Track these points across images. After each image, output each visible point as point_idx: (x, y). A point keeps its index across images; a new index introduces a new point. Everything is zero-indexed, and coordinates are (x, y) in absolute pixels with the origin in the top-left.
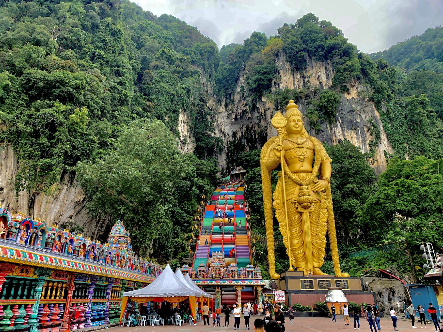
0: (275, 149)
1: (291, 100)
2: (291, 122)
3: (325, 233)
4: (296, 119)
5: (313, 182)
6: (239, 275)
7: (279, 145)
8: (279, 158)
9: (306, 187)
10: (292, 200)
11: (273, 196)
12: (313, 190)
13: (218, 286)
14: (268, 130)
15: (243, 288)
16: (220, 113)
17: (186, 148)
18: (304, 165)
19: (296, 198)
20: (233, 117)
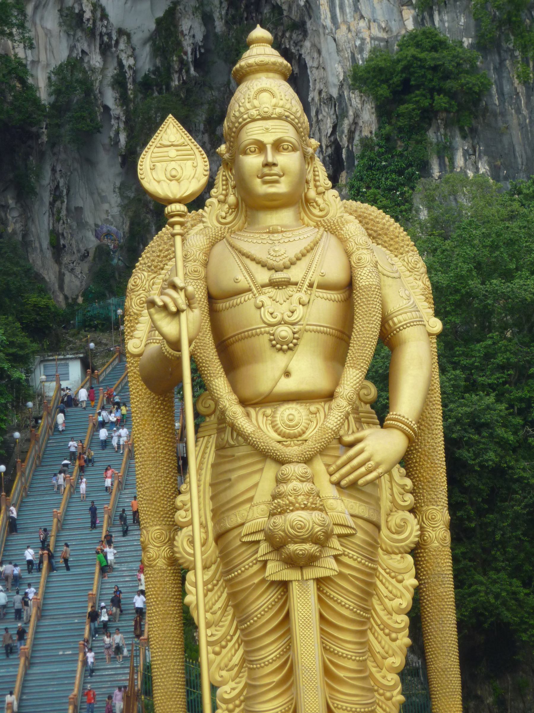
0: (152, 304)
1: (259, 32)
2: (245, 153)
4: (268, 139)
5: (340, 440)
7: (174, 287)
8: (176, 345)
9: (299, 469)
10: (245, 530)
11: (176, 509)
12: (335, 477)
14: (307, 44)
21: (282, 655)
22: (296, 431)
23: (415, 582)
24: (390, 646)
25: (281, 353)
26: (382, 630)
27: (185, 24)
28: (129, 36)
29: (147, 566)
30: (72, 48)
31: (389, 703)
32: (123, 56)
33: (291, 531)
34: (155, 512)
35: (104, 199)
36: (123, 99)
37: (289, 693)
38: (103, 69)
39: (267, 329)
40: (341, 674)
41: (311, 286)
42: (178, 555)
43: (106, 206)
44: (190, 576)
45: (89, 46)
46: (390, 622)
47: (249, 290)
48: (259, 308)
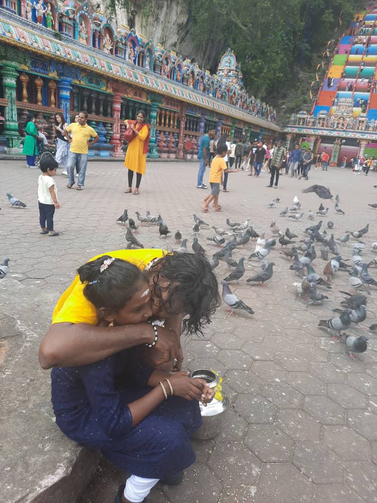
6: (367, 127)
13: (339, 137)
15: (369, 143)
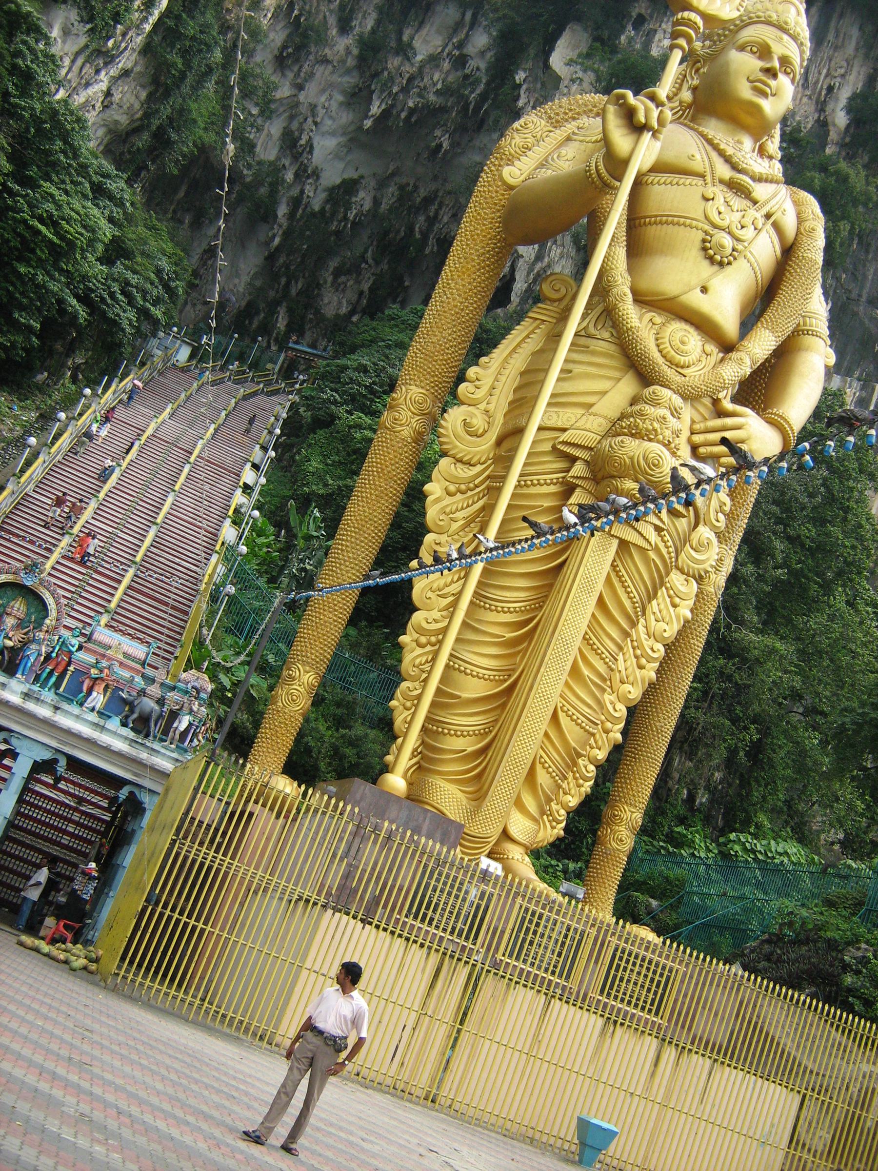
2: (742, 48)
3: (635, 693)
4: (778, 50)
5: (716, 402)
9: (677, 401)
10: (564, 437)
11: (461, 378)
12: (697, 439)
16: (325, 61)
17: (103, 86)
18: (713, 285)
19: (590, 439)
20: (375, 109)
21: (522, 611)
22: (682, 360)
23: (689, 615)
24: (634, 671)
25: (706, 263)
26: (634, 648)
27: (362, 194)
28: (318, 178)
29: (387, 428)
30: (278, 159)
31: (604, 735)
32: (308, 187)
33: (642, 462)
34: (429, 373)
35: (238, 275)
36: (291, 216)
37: (511, 661)
38: (290, 186)
39: (707, 227)
40: (586, 671)
41: (768, 216)
42: (441, 430)
43: (236, 281)
44: (444, 462)
45: (290, 164)
46: (644, 642)
47: (702, 176)
48: (707, 200)
